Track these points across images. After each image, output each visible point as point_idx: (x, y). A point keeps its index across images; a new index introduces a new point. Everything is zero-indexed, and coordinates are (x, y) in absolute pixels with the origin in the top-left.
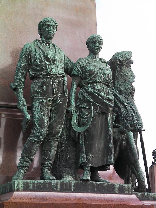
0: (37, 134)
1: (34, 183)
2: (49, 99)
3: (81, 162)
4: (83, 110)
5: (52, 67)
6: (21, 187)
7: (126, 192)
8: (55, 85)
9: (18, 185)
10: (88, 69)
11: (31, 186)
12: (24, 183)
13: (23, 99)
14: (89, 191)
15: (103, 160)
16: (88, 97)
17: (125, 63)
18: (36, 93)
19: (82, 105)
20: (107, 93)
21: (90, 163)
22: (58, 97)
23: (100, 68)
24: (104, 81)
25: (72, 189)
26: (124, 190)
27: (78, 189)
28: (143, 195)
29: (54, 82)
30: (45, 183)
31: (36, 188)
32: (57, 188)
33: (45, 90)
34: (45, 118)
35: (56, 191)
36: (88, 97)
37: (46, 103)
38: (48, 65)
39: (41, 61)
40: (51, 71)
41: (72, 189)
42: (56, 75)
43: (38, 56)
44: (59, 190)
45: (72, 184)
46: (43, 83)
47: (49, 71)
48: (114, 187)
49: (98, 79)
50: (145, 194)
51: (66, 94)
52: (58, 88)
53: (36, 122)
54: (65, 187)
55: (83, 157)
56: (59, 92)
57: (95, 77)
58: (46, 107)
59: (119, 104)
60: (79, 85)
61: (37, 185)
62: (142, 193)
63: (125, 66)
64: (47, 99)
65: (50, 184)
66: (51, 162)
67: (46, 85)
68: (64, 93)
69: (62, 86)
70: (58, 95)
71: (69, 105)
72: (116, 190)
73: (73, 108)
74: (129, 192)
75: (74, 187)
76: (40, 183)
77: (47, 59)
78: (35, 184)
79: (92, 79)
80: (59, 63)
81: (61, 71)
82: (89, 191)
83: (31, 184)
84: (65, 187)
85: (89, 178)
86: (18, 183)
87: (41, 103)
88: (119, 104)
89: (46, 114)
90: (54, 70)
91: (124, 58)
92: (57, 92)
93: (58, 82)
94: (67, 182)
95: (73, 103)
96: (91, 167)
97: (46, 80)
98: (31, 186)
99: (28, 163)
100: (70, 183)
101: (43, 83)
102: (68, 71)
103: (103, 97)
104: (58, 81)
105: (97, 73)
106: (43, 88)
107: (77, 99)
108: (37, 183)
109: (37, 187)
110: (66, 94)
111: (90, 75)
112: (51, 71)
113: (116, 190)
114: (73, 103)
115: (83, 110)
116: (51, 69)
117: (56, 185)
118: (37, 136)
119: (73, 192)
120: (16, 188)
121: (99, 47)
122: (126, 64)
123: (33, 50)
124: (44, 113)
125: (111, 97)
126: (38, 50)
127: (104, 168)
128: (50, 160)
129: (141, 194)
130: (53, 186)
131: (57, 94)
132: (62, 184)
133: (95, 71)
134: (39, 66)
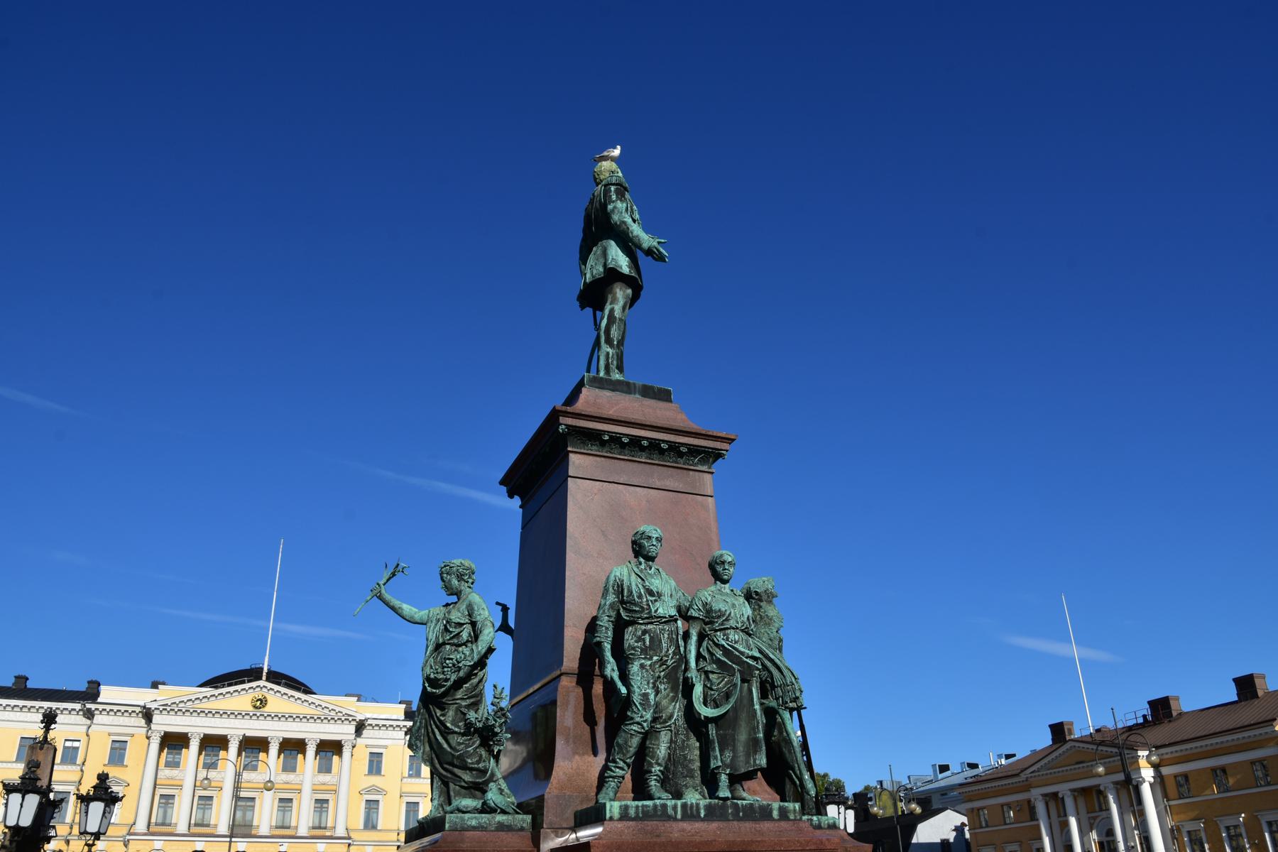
0: (638, 719)
1: (637, 807)
2: (655, 658)
3: (712, 766)
4: (711, 676)
5: (658, 604)
6: (616, 814)
7: (792, 817)
10: (716, 606)
11: (632, 812)
13: (612, 660)
15: (747, 762)
16: (719, 654)
17: (765, 597)
18: (634, 648)
19: (709, 668)
20: (746, 648)
23: (734, 606)
27: (712, 813)
30: (655, 806)
32: (676, 813)
35: (675, 819)
36: (719, 654)
39: (640, 596)
43: (634, 587)
44: (679, 816)
46: (645, 632)
49: (732, 623)
51: (682, 649)
52: (670, 639)
53: (636, 698)
55: (716, 758)
57: (727, 620)
59: (768, 664)
60: (702, 637)
64: (651, 658)
65: (664, 806)
68: (678, 647)
71: (686, 669)
72: (775, 814)
73: (693, 674)
77: (650, 593)
81: (673, 612)
85: (728, 794)
87: (642, 666)
88: (768, 664)
90: (661, 611)
95: (693, 664)
96: (729, 775)
97: (650, 627)
98: (632, 812)
100: (698, 805)
101: (645, 632)
102: (683, 613)
106: (644, 640)
107: (699, 656)
110: (682, 649)
111: (719, 617)
113: (775, 814)
114: (693, 664)
115: (711, 676)
117: (675, 807)
118: (638, 723)
119: (703, 820)
120: (608, 816)
123: (625, 579)
125: (758, 655)
126: (633, 576)
127: (750, 776)
128: (659, 765)
130: (670, 811)
132: (684, 806)
134: (635, 604)
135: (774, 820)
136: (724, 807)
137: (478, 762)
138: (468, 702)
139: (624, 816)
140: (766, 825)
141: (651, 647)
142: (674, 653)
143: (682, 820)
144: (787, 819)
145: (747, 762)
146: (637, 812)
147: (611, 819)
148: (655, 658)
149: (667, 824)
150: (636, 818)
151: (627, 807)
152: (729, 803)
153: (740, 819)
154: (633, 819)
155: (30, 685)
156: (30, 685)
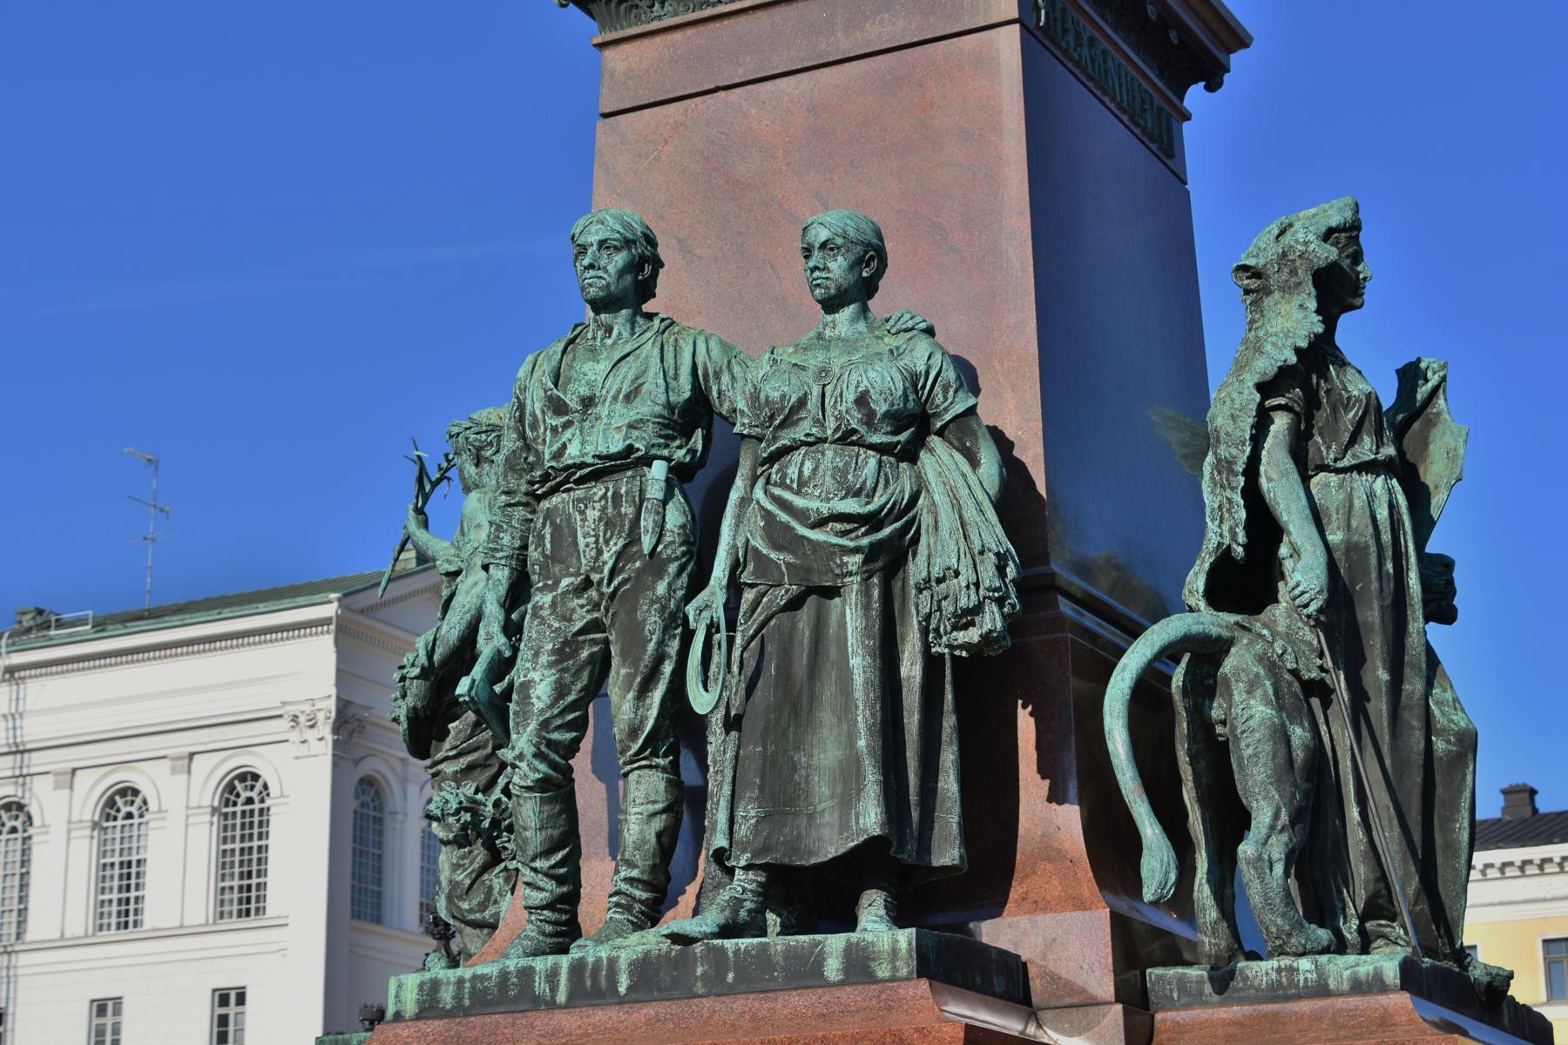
2: (565, 582)
5: (568, 434)
7: (883, 972)
8: (582, 513)
9: (397, 996)
11: (447, 997)
12: (421, 985)
14: (699, 988)
15: (844, 826)
21: (744, 851)
22: (605, 563)
24: (835, 431)
25: (622, 989)
26: (873, 960)
28: (1292, 970)
29: (580, 500)
30: (504, 975)
31: (467, 1002)
32: (554, 989)
33: (548, 546)
34: (535, 676)
35: (552, 1005)
37: (554, 604)
38: (554, 430)
40: (558, 455)
41: (622, 989)
42: (586, 465)
44: (561, 997)
45: (623, 964)
47: (547, 457)
48: (822, 952)
49: (799, 433)
50: (1305, 964)
54: (589, 983)
56: (607, 542)
58: (550, 626)
61: (473, 987)
62: (1285, 961)
63: (1282, 289)
64: (557, 583)
66: (635, 873)
67: (553, 524)
69: (627, 510)
70: (606, 556)
72: (833, 968)
74: (895, 968)
75: (631, 975)
76: (483, 978)
77: (558, 407)
78: (467, 985)
79: (775, 439)
80: (619, 406)
82: (699, 988)
83: (448, 983)
84: (589, 983)
86: (400, 986)
89: (544, 659)
90: (573, 450)
91: (1274, 250)
92: (597, 542)
93: (604, 496)
94: (598, 961)
98: (447, 997)
99: (541, 889)
100: (613, 962)
103: (800, 515)
104: (607, 489)
105: (802, 402)
108: (475, 978)
109: (473, 994)
112: (558, 455)
113: (833, 968)
116: (559, 445)
119: (622, 1001)
121: (826, 269)
122: (1285, 276)
124: (536, 655)
129: (1279, 970)
130: (541, 986)
131: (600, 552)
132: (577, 969)
133: (783, 396)
135: (829, 985)
136: (681, 965)
137: (483, 906)
138: (464, 762)
139: (429, 1007)
140: (798, 1001)
141: (554, 558)
142: (619, 556)
143: (568, 1005)
144: (871, 978)
145: (844, 826)
146: (458, 997)
147: (398, 1017)
148: (565, 582)
149: (522, 1020)
150: (458, 1011)
151: (435, 985)
152: (698, 948)
153: (731, 991)
154: (449, 1014)
155: (1544, 805)
156: (1544, 805)
